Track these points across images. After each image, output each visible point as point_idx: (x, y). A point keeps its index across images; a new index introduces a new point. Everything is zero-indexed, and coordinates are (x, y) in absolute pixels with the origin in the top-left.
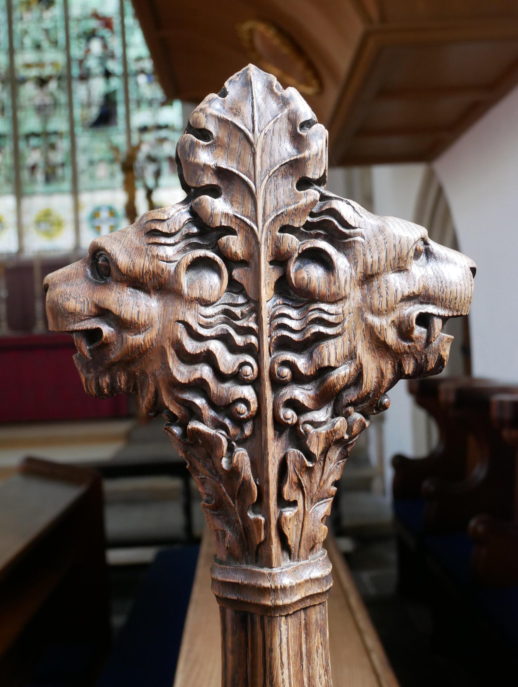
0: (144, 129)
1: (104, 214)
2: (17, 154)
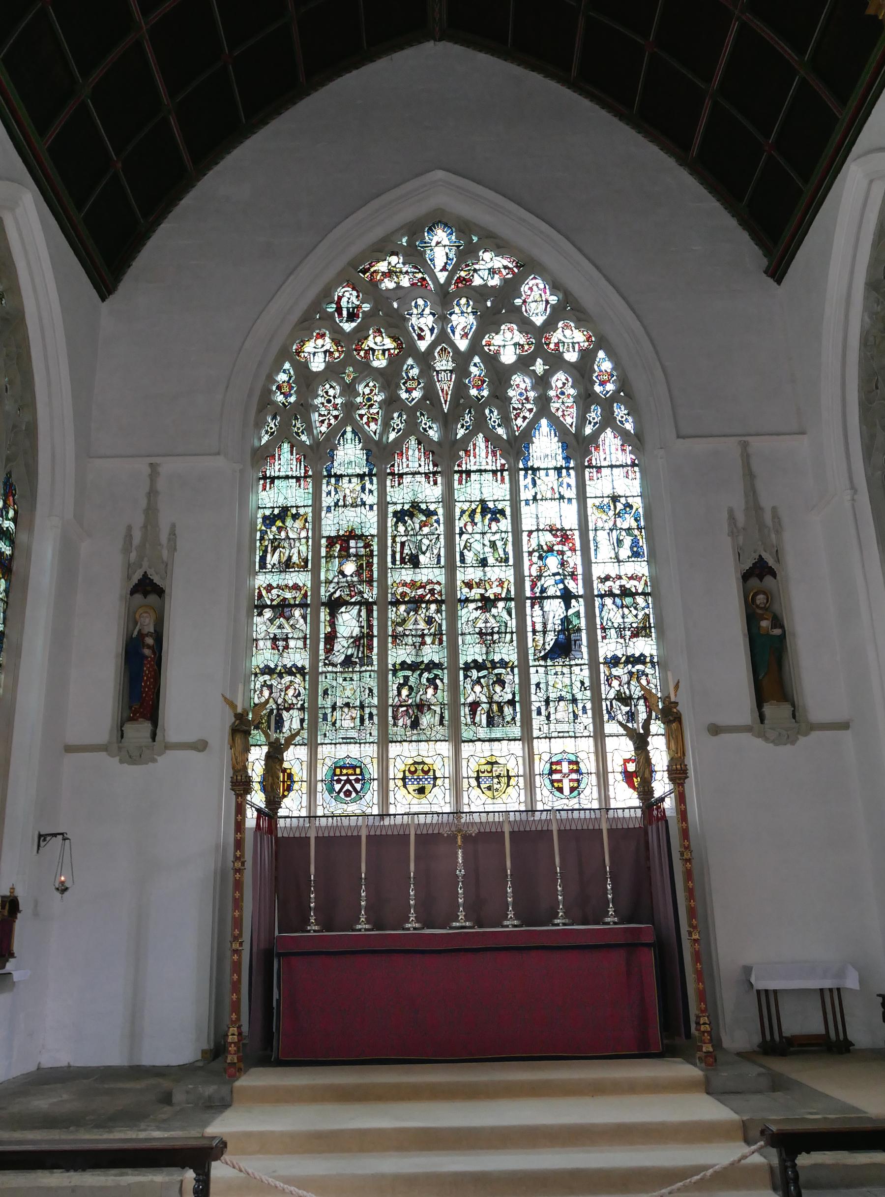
0: (614, 661)
1: (565, 767)
2: (454, 689)
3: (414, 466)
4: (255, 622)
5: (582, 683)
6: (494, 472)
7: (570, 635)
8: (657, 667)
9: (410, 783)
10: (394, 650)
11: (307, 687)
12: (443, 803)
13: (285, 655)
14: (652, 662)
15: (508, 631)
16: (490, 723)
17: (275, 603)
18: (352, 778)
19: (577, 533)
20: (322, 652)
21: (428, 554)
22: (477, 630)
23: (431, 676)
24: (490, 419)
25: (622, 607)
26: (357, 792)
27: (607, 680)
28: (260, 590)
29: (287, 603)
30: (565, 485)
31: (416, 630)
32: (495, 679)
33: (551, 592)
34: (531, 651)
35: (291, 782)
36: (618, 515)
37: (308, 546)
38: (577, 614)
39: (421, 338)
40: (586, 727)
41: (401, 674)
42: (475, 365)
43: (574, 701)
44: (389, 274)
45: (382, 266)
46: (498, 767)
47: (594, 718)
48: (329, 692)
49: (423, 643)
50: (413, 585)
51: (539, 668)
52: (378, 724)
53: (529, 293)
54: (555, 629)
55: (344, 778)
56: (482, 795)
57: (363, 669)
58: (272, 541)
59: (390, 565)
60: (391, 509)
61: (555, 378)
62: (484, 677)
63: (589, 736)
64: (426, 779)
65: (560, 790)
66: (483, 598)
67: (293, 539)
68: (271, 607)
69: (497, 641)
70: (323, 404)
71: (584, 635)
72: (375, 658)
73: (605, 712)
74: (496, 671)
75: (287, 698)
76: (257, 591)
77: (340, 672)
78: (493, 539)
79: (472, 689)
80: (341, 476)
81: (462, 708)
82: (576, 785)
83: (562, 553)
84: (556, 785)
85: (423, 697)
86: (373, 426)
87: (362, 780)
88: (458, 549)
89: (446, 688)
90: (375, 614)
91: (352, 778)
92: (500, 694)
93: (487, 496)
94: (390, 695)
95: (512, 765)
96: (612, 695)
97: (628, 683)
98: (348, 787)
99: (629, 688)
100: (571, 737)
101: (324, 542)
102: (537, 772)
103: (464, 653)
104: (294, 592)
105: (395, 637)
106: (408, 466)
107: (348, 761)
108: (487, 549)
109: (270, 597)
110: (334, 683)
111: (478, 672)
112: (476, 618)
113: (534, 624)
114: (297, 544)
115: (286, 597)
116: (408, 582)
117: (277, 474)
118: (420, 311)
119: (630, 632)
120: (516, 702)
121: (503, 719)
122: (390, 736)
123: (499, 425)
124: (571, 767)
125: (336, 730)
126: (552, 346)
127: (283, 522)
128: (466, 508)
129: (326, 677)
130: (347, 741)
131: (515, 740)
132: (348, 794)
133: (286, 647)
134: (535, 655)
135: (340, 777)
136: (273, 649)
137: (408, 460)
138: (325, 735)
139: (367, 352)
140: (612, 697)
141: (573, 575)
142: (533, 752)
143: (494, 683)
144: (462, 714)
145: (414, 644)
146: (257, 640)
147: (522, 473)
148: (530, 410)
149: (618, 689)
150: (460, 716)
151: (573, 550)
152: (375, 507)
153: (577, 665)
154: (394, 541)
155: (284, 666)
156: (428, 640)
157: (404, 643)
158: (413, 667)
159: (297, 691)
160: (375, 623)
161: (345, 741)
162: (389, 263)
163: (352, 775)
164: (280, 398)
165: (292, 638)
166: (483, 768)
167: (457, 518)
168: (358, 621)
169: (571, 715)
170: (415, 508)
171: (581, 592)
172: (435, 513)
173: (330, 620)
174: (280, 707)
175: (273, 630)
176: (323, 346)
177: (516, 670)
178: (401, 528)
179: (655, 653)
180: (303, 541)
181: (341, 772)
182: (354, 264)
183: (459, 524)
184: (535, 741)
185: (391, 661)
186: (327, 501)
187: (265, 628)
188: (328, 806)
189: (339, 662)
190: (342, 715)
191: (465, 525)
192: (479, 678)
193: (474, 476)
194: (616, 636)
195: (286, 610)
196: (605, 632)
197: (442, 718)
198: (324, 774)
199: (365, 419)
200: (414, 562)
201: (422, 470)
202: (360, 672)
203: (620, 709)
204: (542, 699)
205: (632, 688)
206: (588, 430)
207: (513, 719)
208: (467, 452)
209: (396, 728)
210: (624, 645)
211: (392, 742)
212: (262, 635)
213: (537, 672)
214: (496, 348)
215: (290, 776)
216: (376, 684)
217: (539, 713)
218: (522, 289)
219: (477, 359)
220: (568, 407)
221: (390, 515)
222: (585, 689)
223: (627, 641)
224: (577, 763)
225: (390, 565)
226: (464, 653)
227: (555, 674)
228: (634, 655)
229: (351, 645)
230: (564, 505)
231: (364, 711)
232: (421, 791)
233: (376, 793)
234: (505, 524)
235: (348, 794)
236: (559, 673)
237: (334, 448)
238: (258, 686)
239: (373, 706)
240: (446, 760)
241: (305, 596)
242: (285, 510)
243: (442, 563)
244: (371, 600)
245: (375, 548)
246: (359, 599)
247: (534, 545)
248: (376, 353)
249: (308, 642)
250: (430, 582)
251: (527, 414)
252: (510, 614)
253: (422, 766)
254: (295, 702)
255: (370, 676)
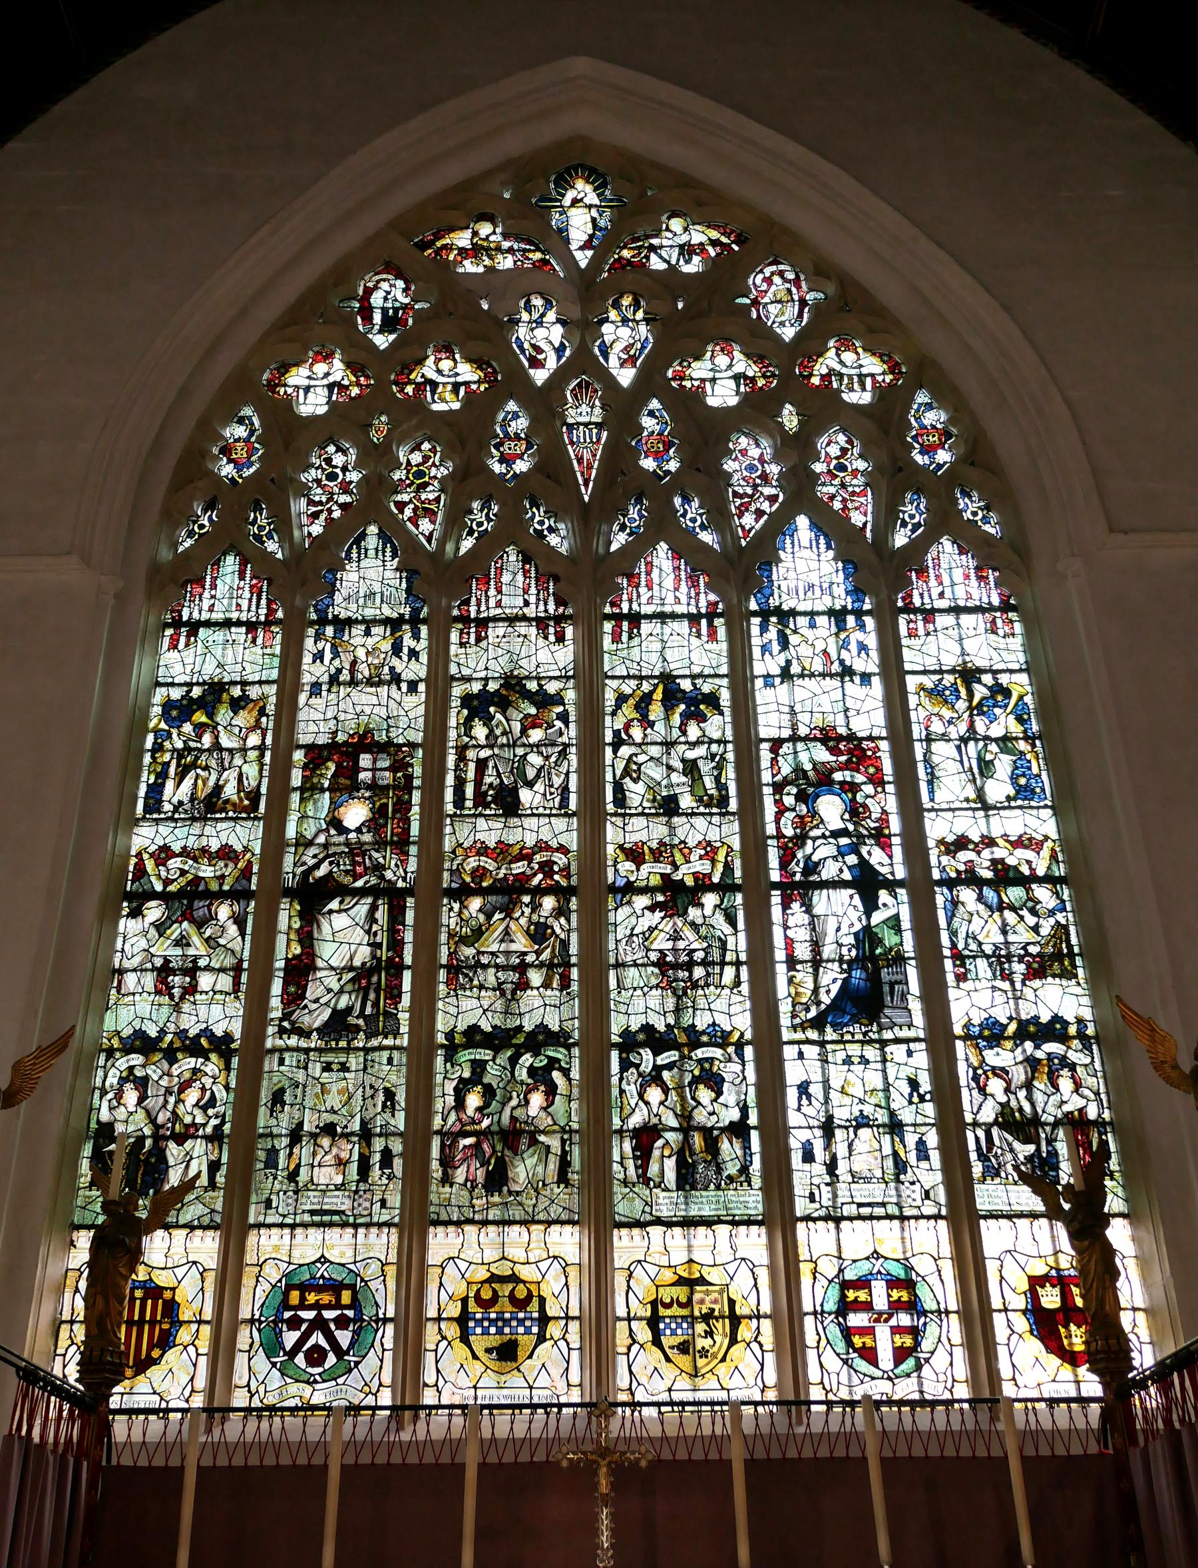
1: (880, 1296)
3: (513, 603)
4: (121, 929)
5: (914, 1084)
6: (694, 619)
7: (877, 971)
8: (1095, 1047)
9: (479, 1330)
10: (453, 1000)
11: (233, 1085)
12: (561, 1386)
13: (186, 1007)
14: (1081, 1036)
15: (728, 959)
16: (687, 1180)
17: (172, 888)
18: (329, 1314)
19: (884, 745)
20: (275, 1002)
21: (539, 787)
22: (654, 956)
23: (541, 1062)
24: (684, 515)
25: (1001, 907)
26: (340, 1353)
27: (976, 1078)
28: (142, 860)
29: (201, 888)
30: (853, 647)
31: (508, 953)
32: (697, 1072)
33: (829, 871)
34: (785, 1008)
35: (172, 1324)
36: (977, 709)
37: (262, 765)
38: (894, 923)
39: (536, 363)
40: (927, 1193)
41: (465, 1056)
42: (651, 414)
43: (895, 1127)
44: (476, 251)
45: (463, 239)
46: (707, 1293)
47: (947, 1169)
48: (288, 1098)
49: (524, 985)
50: (502, 852)
51: (805, 1048)
52: (403, 1179)
53: (764, 287)
54: (841, 956)
55: (309, 1315)
56: (664, 1366)
57: (374, 1042)
58: (180, 754)
59: (449, 808)
60: (457, 691)
61: (824, 440)
62: (670, 1066)
63: (937, 1217)
64: (521, 1322)
65: (870, 1355)
66: (669, 884)
67: (230, 751)
68: (164, 897)
69: (702, 983)
70: (318, 481)
71: (912, 973)
72: (404, 1017)
73: (973, 1156)
74: (700, 1053)
75: (181, 1110)
76: (133, 861)
77: (315, 1049)
78: (691, 755)
79: (641, 1096)
80: (350, 622)
81: (615, 1141)
82: (908, 1341)
83: (851, 788)
84: (857, 1341)
85: (517, 1113)
86: (425, 525)
87: (355, 1321)
88: (609, 777)
89: (576, 1091)
90: (410, 917)
91: (329, 1314)
92: (710, 1109)
93: (676, 665)
94: (439, 1106)
95: (741, 1286)
96: (988, 1114)
97: (1028, 1085)
98: (317, 1338)
99: (1029, 1098)
100: (890, 1217)
101: (298, 756)
102: (807, 1306)
103: (623, 1008)
104: (221, 864)
105: (455, 969)
106: (499, 604)
107: (322, 1270)
108: (676, 778)
109: (163, 874)
110: (300, 1076)
111: (655, 1054)
112: (652, 929)
113: (789, 943)
114: (238, 761)
115: (201, 874)
116: (492, 845)
117: (205, 616)
118: (535, 316)
119: (1023, 966)
120: (749, 1128)
121: (719, 1170)
122: (432, 1209)
123: (703, 527)
124: (895, 1294)
125: (296, 1192)
126: (816, 381)
127: (211, 716)
128: (628, 691)
129: (281, 1062)
130: (324, 1219)
131: (749, 1222)
132: (316, 1357)
133: (191, 989)
134: (794, 1016)
135: (299, 1313)
136: (158, 992)
137: (499, 591)
138: (268, 1204)
139: (419, 387)
140: (991, 1119)
141: (881, 838)
142: (797, 1255)
143: (696, 1081)
144: (616, 1157)
145: (499, 987)
146: (121, 972)
147: (756, 621)
148: (772, 499)
149: (1004, 1099)
150: (611, 1161)
151: (877, 781)
152: (422, 687)
153: (897, 1041)
154: (461, 758)
155: (182, 1034)
156: (536, 978)
157: (476, 982)
158: (497, 1040)
159: (208, 1093)
160: (409, 936)
161: (317, 1218)
162: (475, 234)
163: (329, 1307)
164: (228, 470)
165: (208, 968)
166: (667, 1295)
167: (609, 710)
168: (368, 932)
169: (889, 1163)
170: (513, 685)
171: (900, 873)
172: (558, 699)
173: (301, 927)
174: (161, 1132)
175: (164, 949)
176: (327, 375)
177: (749, 1052)
178: (480, 732)
179: (1087, 1014)
180: (253, 755)
181: (303, 1298)
182: (401, 225)
183: (611, 725)
184: (801, 1226)
185: (442, 1024)
186: (312, 672)
187: (143, 944)
188: (261, 1389)
189: (316, 1025)
190: (314, 1154)
191: (627, 726)
192: (658, 1069)
193: (646, 627)
194: (989, 975)
195: (197, 904)
196: (963, 965)
197: (564, 1164)
198: (257, 1306)
199: (408, 512)
200: (508, 804)
201: (530, 612)
202: (366, 1050)
203: (1012, 1150)
204: (816, 1123)
205: (1039, 1097)
206: (901, 539)
207: (744, 1170)
208: (631, 577)
209: (447, 1189)
210: (1010, 994)
211: (437, 1223)
212: (135, 962)
213: (801, 1055)
214: (696, 383)
215: (171, 1307)
216: (403, 1081)
217: (808, 1157)
218: (750, 281)
219: (655, 404)
220: (853, 493)
221: (455, 703)
222: (922, 1099)
223: (1018, 986)
224: (908, 1284)
225: (449, 808)
226: (623, 1008)
227: (844, 1062)
228: (1037, 1018)
229: (349, 988)
230: (853, 688)
231: (369, 1145)
232: (507, 1353)
233: (388, 1355)
234: (718, 725)
235: (316, 1357)
236: (856, 1060)
237: (337, 567)
238: (112, 1080)
239: (394, 1134)
240: (573, 1272)
241: (246, 873)
242: (215, 690)
243: (573, 805)
244: (400, 884)
245: (418, 771)
246: (374, 881)
247: (786, 770)
248: (440, 389)
249: (244, 978)
250: (542, 846)
251: (765, 506)
252: (731, 921)
253: (511, 1286)
254: (200, 1119)
255: (390, 1061)
